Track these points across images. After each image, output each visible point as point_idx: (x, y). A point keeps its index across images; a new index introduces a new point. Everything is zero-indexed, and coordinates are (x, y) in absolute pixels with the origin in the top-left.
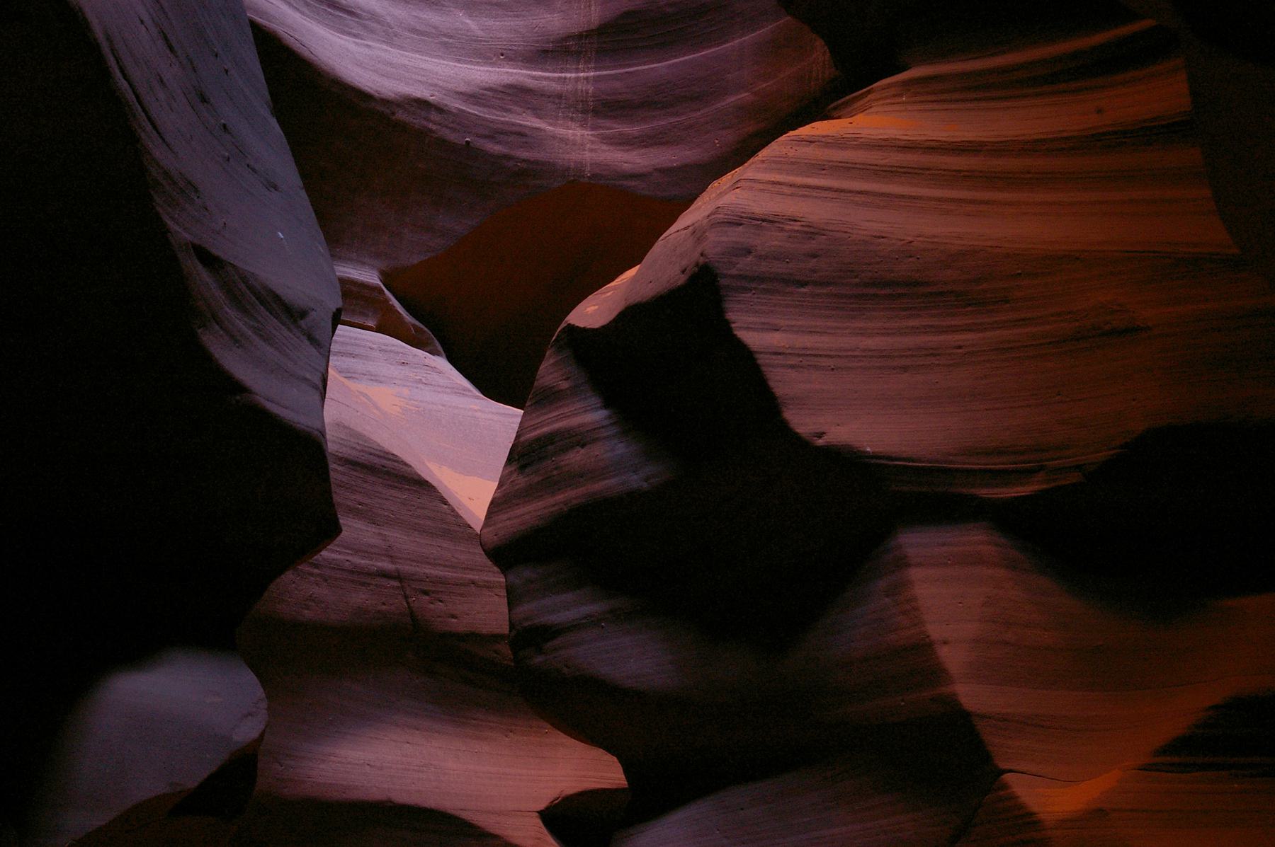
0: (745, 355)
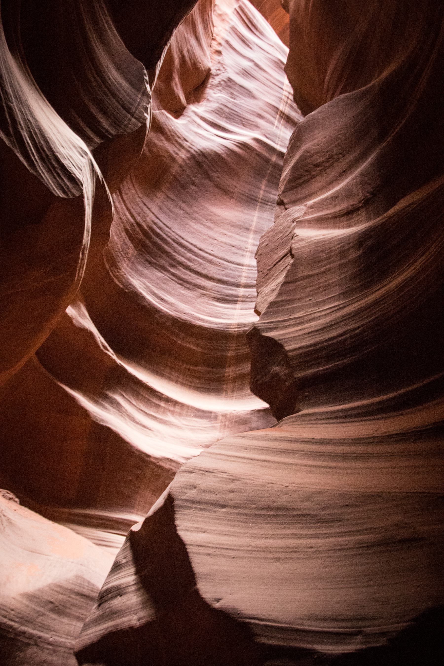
0: (181, 545)
